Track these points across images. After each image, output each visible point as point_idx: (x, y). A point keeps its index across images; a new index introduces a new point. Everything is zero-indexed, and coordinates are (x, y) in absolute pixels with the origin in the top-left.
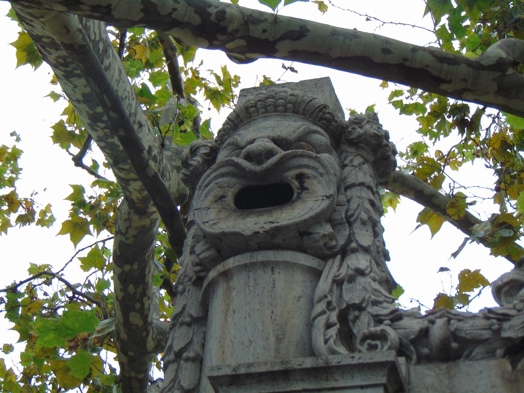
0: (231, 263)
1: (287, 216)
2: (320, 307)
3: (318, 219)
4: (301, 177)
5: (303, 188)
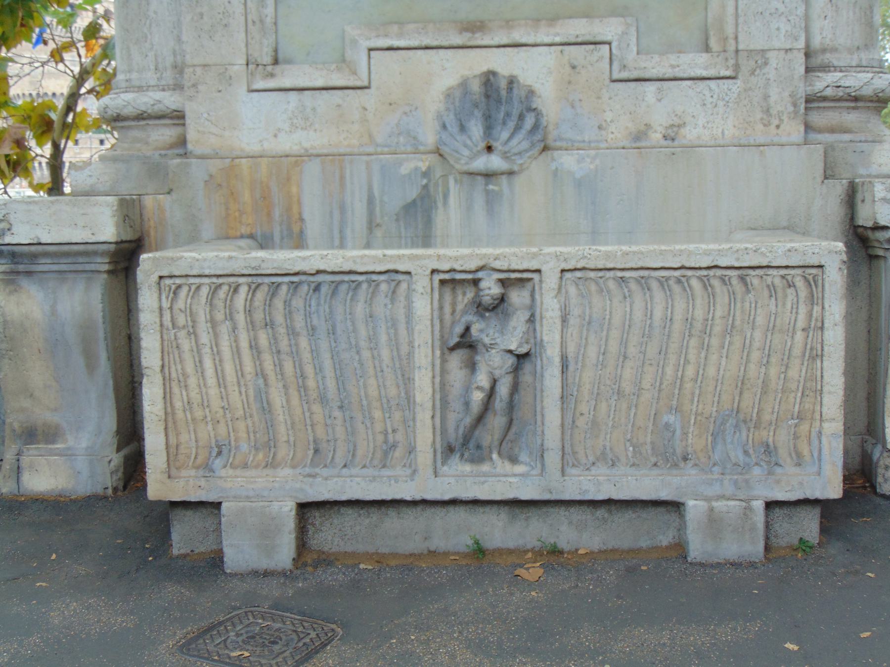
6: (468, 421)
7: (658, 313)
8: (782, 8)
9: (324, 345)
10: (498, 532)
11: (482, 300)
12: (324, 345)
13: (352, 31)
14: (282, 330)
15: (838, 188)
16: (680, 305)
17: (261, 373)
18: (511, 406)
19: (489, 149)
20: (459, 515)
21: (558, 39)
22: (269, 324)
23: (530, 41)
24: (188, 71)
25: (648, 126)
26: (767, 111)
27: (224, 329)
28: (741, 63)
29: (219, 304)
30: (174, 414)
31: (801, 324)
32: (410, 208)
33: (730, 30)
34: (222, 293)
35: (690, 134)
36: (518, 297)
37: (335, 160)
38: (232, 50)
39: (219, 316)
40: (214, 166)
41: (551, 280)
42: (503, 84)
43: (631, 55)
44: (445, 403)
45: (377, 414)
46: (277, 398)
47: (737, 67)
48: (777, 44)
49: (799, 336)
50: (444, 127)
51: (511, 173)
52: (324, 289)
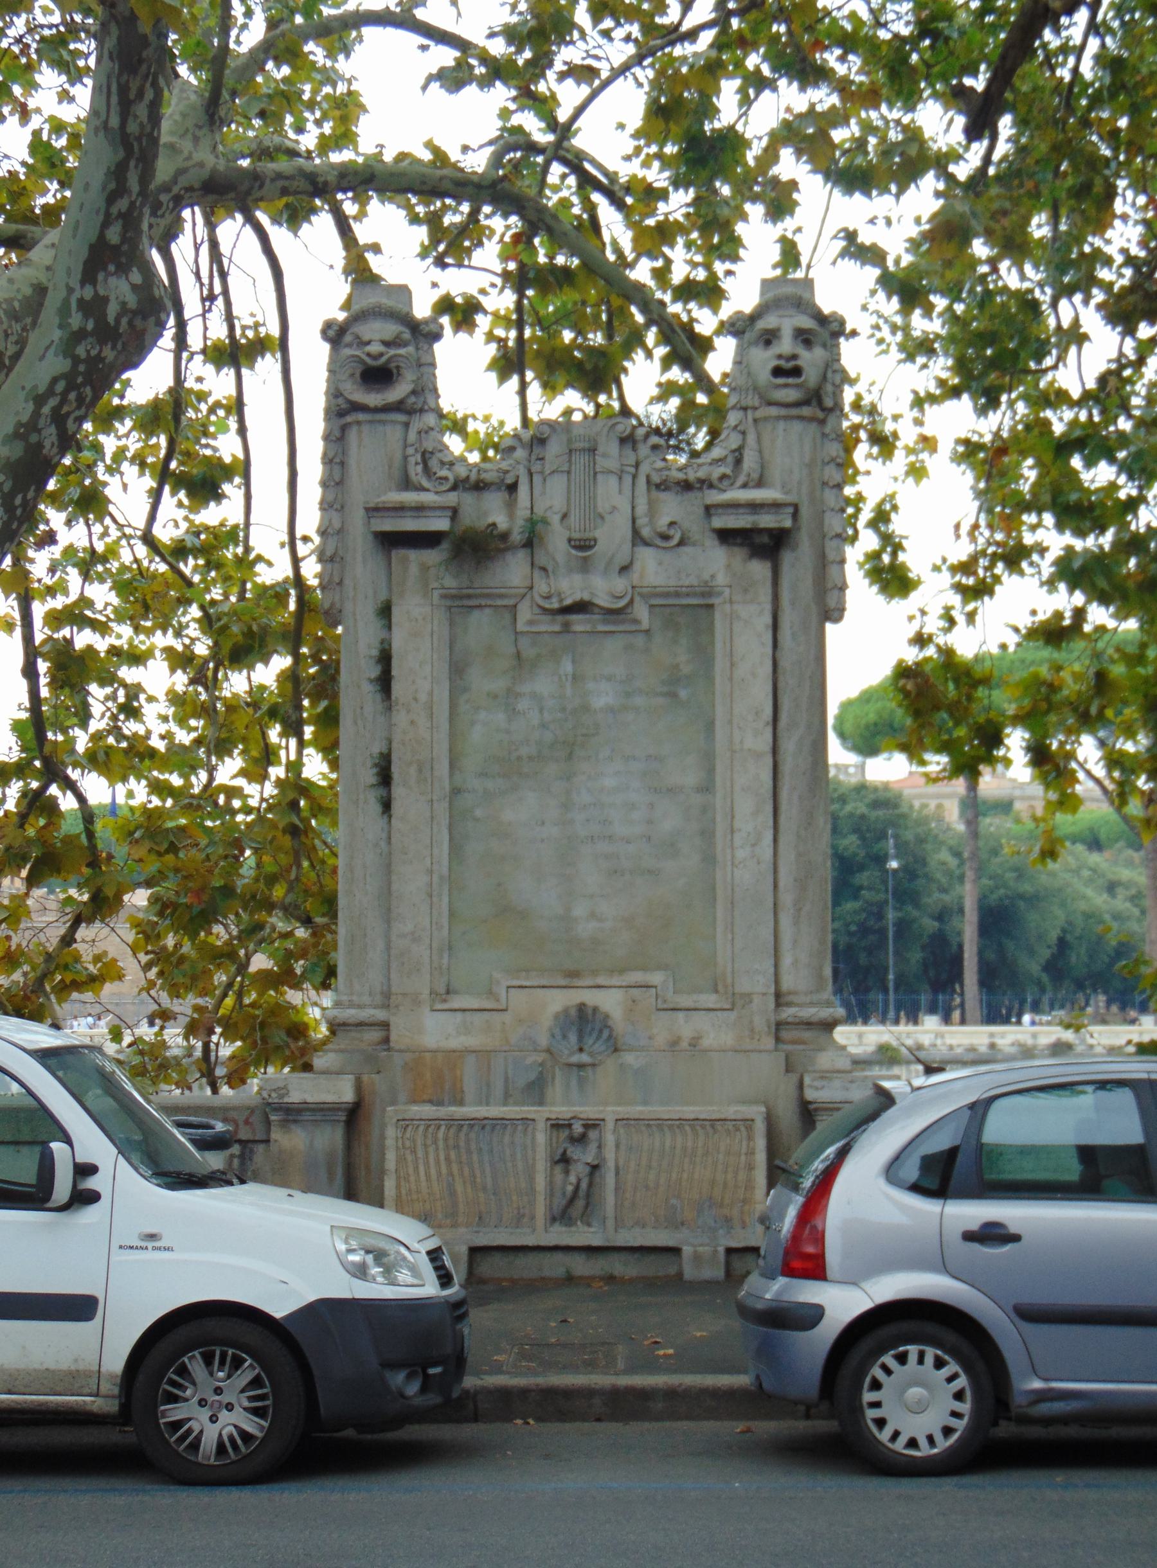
2: (410, 451)
4: (398, 367)
5: (399, 374)
6: (564, 1202)
7: (668, 1144)
9: (486, 1158)
10: (581, 1266)
11: (574, 1135)
12: (486, 1158)
13: (497, 975)
14: (463, 1150)
15: (794, 1078)
16: (679, 1140)
18: (588, 1195)
19: (581, 1050)
20: (559, 1256)
22: (457, 1147)
24: (393, 997)
26: (752, 1030)
27: (431, 1150)
28: (737, 1001)
31: (744, 1150)
32: (531, 1086)
33: (729, 980)
35: (706, 1042)
36: (593, 1134)
37: (484, 1055)
38: (422, 985)
39: (429, 1142)
40: (408, 1056)
41: (610, 1125)
42: (590, 1012)
44: (552, 1195)
45: (514, 1198)
46: (459, 1188)
47: (733, 1004)
49: (743, 1158)
50: (553, 1036)
51: (594, 1065)
52: (488, 1128)
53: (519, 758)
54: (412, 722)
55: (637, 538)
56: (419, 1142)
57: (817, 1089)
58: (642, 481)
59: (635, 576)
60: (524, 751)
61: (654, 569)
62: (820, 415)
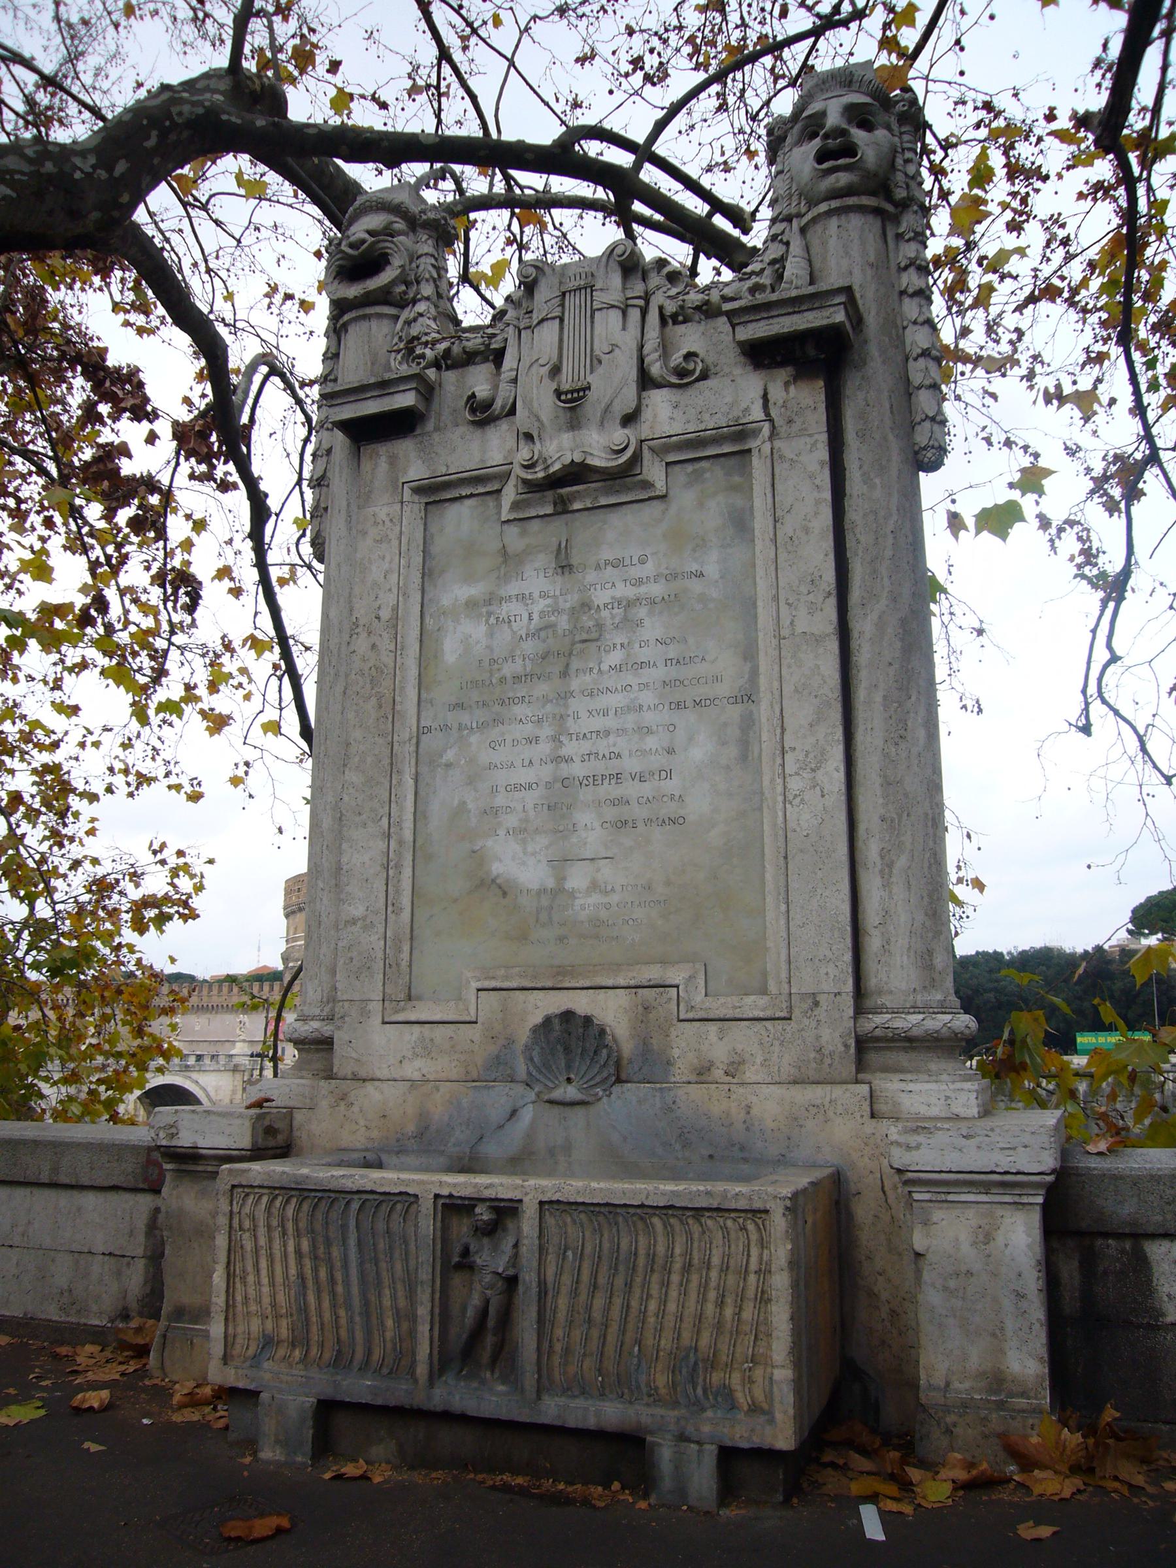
0: (346, 318)
1: (374, 283)
3: (393, 283)
8: (829, 954)
17: (301, 1276)
21: (632, 983)
23: (610, 983)
25: (712, 1063)
27: (276, 1234)
29: (275, 1211)
30: (234, 1306)
34: (278, 1203)
39: (275, 1223)
43: (699, 998)
48: (825, 987)
53: (503, 680)
54: (374, 646)
55: (646, 381)
56: (261, 1223)
57: (908, 1148)
58: (653, 317)
59: (645, 429)
60: (508, 670)
61: (665, 414)
62: (890, 208)
